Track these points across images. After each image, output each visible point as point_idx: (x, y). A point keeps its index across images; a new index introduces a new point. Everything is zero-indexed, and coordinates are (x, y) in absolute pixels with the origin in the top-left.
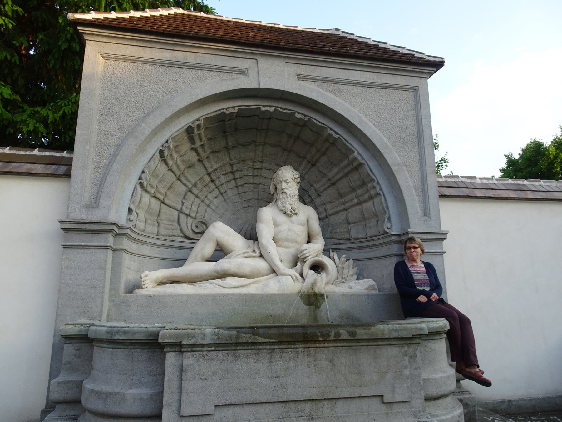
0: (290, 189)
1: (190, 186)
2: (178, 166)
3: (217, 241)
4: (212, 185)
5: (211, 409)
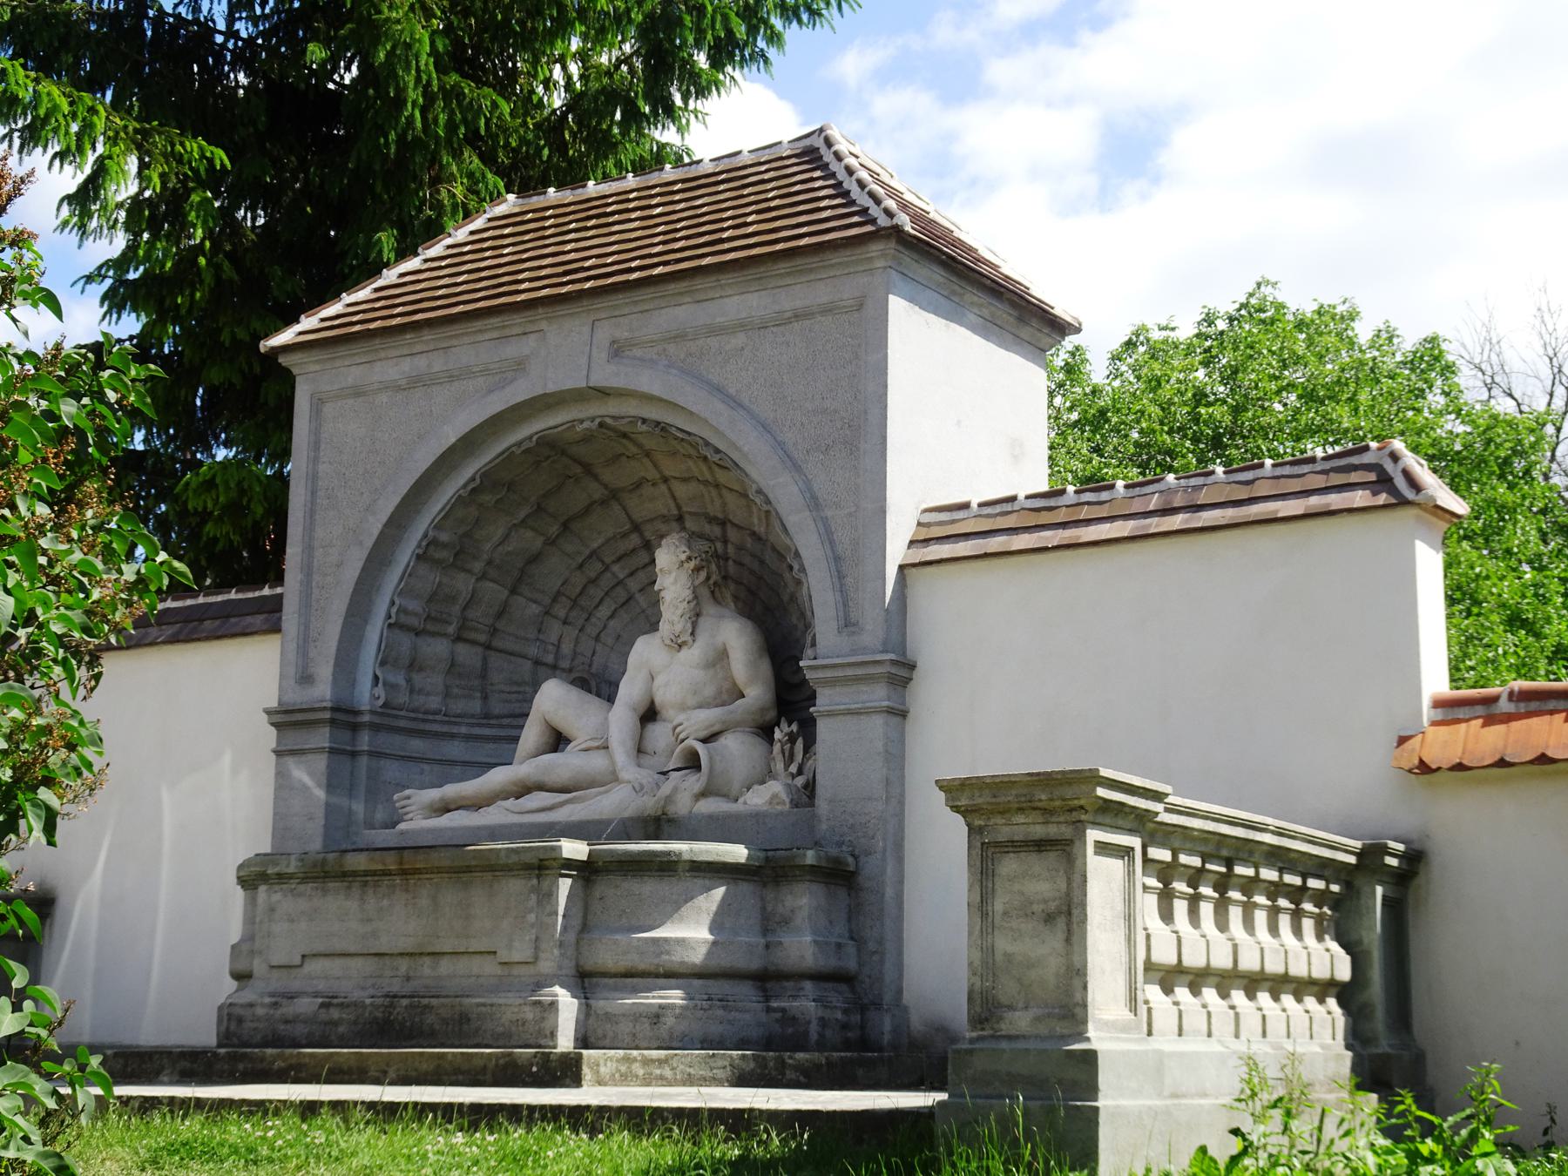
5: (297, 961)
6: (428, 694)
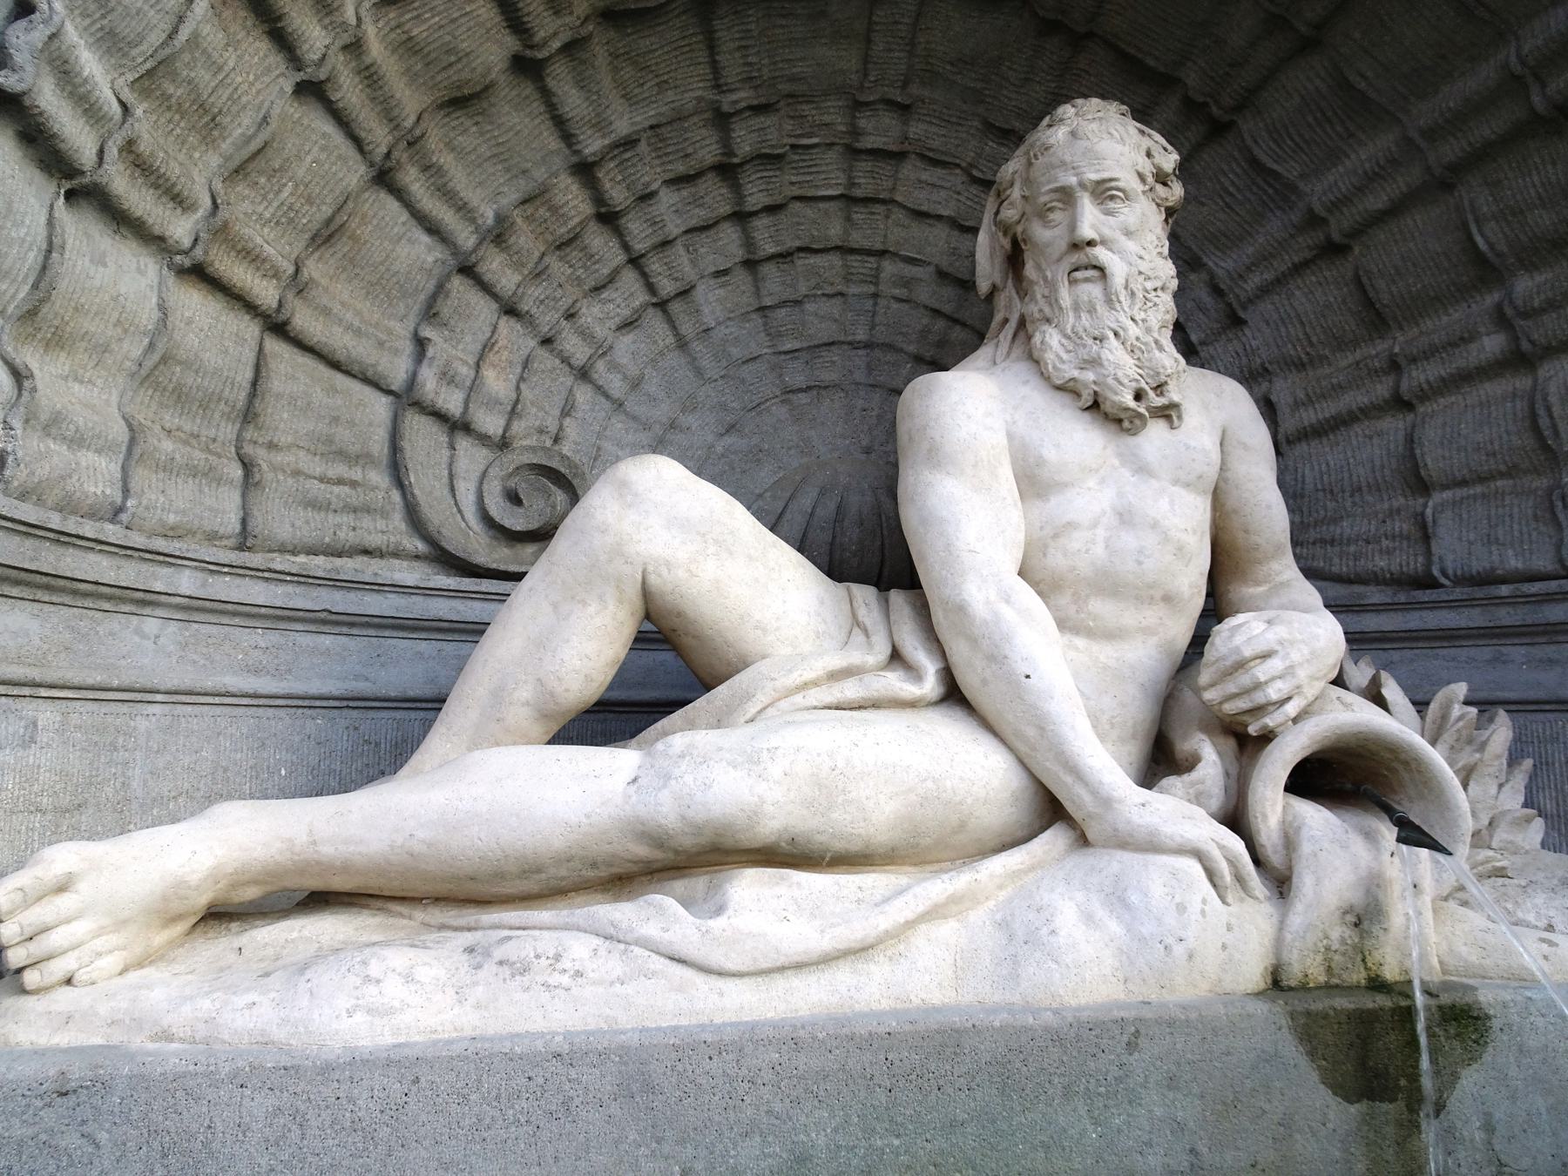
0: (1131, 246)
1: (466, 238)
2: (370, 77)
3: (646, 594)
4: (599, 241)
6: (77, 441)
